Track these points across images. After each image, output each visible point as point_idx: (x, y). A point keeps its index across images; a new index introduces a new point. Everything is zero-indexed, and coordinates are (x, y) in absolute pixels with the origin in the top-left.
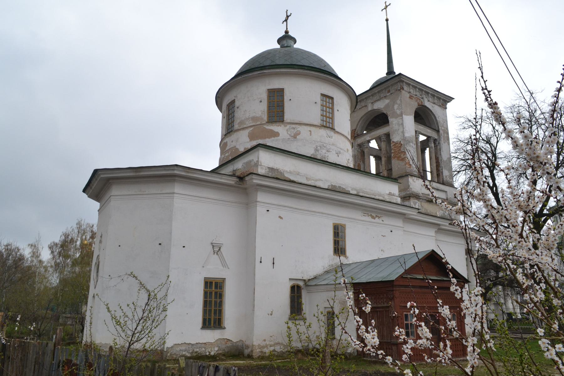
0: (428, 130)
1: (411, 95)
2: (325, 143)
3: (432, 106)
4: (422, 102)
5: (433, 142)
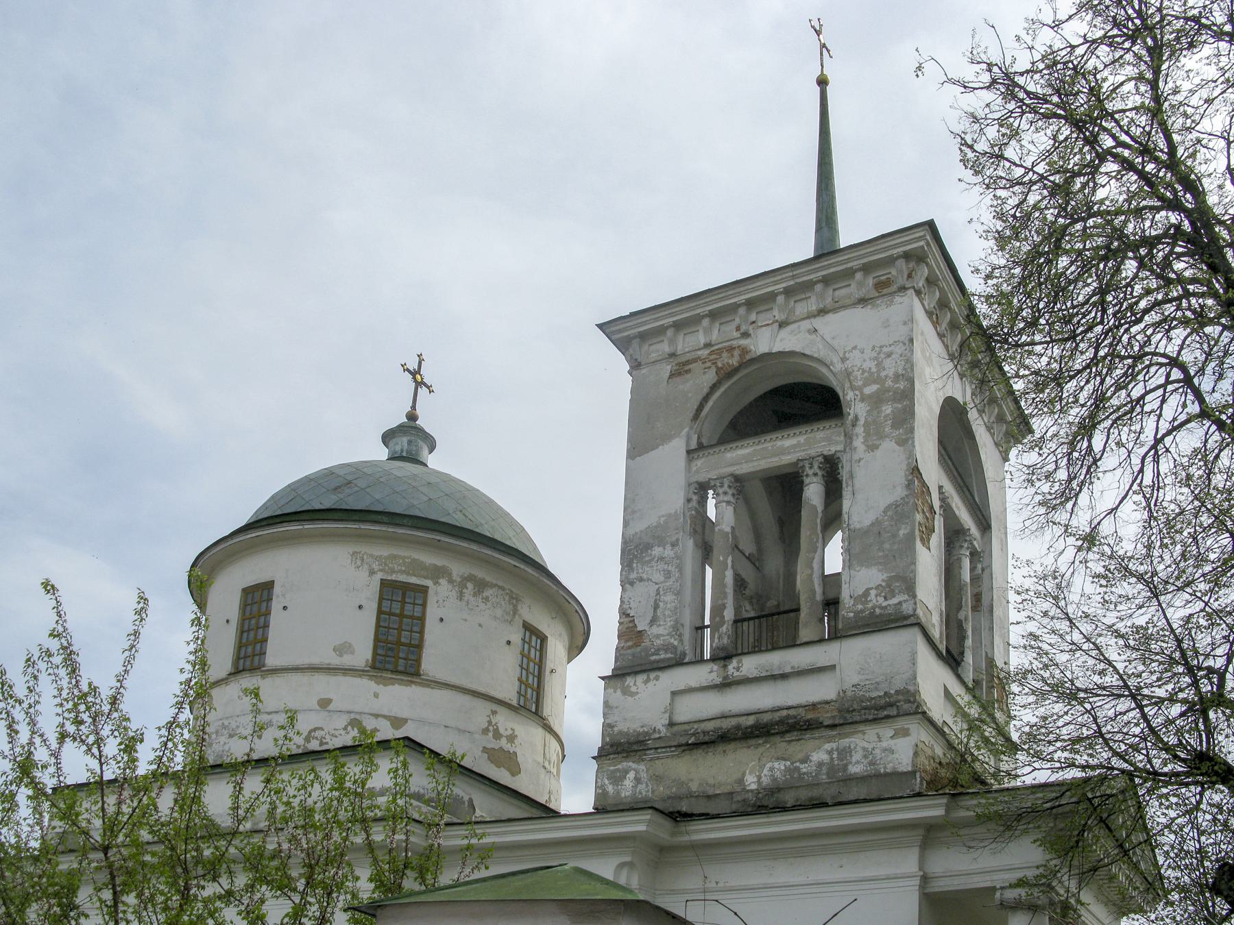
0: (779, 443)
1: (684, 359)
2: (227, 718)
3: (809, 331)
4: (744, 351)
5: (819, 479)
